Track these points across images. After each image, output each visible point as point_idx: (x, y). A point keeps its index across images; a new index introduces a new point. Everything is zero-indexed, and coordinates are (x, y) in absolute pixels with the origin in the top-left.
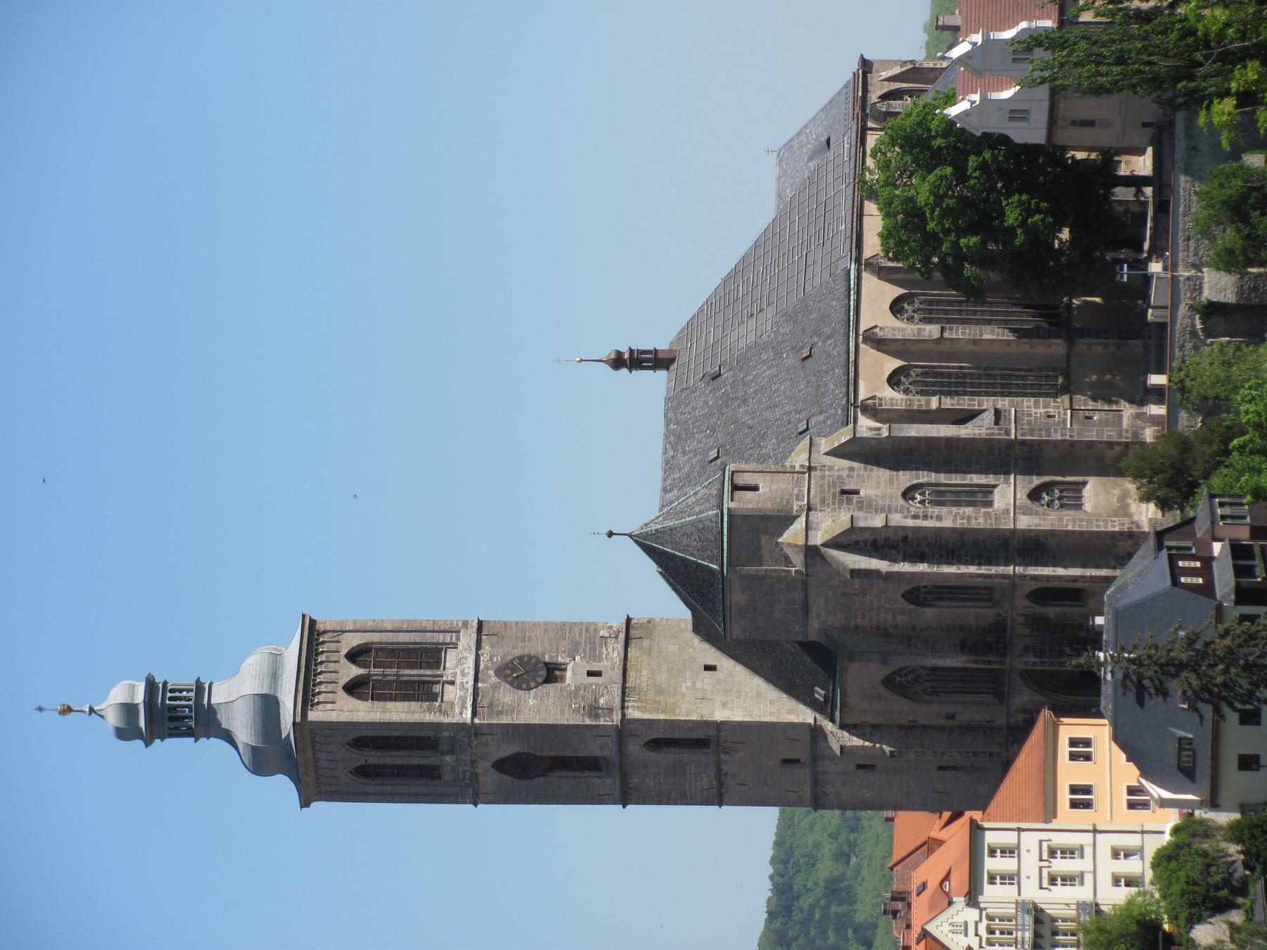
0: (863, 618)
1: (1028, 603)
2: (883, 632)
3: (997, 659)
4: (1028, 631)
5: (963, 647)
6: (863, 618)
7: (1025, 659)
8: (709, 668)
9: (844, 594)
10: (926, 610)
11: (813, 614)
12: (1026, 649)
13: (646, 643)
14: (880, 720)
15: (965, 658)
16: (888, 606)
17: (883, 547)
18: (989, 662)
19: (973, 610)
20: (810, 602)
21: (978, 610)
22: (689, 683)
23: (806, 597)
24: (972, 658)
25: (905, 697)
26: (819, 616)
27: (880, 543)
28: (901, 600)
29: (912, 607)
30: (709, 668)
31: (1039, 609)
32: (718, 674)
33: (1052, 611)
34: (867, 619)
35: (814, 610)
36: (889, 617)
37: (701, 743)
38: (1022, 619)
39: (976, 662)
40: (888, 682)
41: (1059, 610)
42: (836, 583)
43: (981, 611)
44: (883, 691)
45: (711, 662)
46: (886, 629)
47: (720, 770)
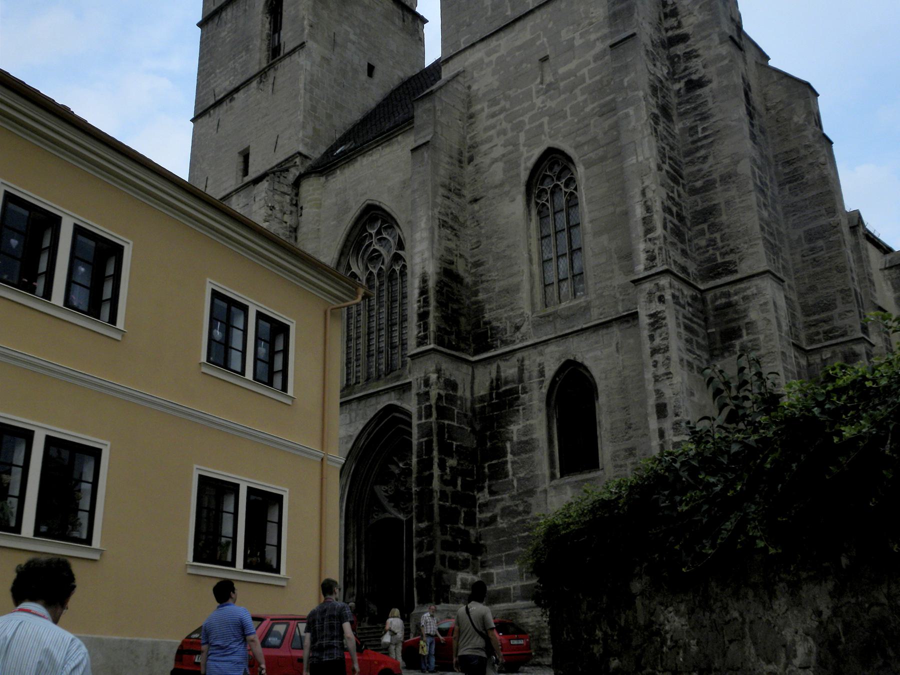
0: (493, 115)
1: (550, 373)
2: (466, 156)
3: (432, 327)
4: (482, 390)
5: (449, 276)
6: (493, 115)
7: (433, 377)
8: (371, 70)
9: (545, 59)
10: (520, 199)
11: (493, 43)
12: (451, 385)
13: (398, 22)
14: (303, 230)
15: (432, 269)
16: (522, 137)
17: (673, 60)
18: (423, 316)
19: (526, 277)
20: (518, 26)
21: (526, 286)
22: (352, 37)
23: (531, 12)
24: (431, 284)
25: (342, 253)
26: (489, 54)
27: (680, 49)
28: (537, 152)
29: (524, 176)
30: (371, 70)
31: (535, 398)
32: (364, 76)
33: (533, 423)
34: (492, 121)
35: (504, 42)
36: (498, 152)
37: (275, 53)
38: (509, 370)
39: (424, 292)
40: (373, 216)
41: (540, 434)
42: (565, 35)
43: (524, 294)
44: (355, 211)
45: (377, 73)
46: (471, 160)
47: (237, 90)
